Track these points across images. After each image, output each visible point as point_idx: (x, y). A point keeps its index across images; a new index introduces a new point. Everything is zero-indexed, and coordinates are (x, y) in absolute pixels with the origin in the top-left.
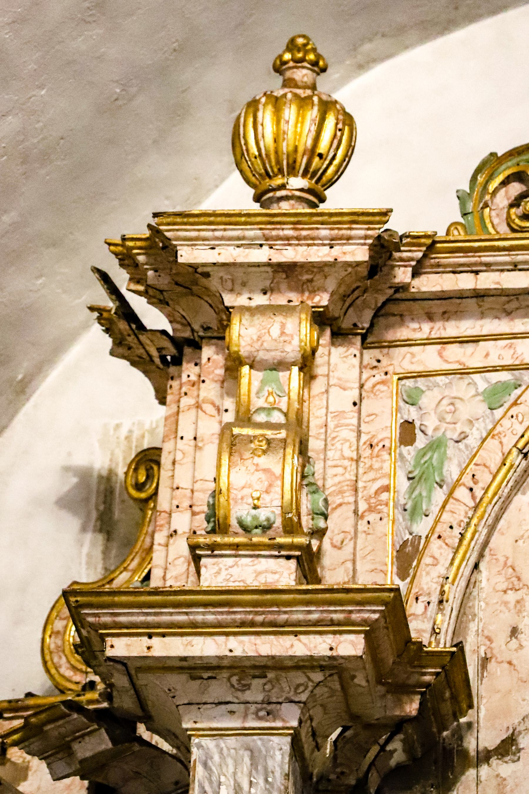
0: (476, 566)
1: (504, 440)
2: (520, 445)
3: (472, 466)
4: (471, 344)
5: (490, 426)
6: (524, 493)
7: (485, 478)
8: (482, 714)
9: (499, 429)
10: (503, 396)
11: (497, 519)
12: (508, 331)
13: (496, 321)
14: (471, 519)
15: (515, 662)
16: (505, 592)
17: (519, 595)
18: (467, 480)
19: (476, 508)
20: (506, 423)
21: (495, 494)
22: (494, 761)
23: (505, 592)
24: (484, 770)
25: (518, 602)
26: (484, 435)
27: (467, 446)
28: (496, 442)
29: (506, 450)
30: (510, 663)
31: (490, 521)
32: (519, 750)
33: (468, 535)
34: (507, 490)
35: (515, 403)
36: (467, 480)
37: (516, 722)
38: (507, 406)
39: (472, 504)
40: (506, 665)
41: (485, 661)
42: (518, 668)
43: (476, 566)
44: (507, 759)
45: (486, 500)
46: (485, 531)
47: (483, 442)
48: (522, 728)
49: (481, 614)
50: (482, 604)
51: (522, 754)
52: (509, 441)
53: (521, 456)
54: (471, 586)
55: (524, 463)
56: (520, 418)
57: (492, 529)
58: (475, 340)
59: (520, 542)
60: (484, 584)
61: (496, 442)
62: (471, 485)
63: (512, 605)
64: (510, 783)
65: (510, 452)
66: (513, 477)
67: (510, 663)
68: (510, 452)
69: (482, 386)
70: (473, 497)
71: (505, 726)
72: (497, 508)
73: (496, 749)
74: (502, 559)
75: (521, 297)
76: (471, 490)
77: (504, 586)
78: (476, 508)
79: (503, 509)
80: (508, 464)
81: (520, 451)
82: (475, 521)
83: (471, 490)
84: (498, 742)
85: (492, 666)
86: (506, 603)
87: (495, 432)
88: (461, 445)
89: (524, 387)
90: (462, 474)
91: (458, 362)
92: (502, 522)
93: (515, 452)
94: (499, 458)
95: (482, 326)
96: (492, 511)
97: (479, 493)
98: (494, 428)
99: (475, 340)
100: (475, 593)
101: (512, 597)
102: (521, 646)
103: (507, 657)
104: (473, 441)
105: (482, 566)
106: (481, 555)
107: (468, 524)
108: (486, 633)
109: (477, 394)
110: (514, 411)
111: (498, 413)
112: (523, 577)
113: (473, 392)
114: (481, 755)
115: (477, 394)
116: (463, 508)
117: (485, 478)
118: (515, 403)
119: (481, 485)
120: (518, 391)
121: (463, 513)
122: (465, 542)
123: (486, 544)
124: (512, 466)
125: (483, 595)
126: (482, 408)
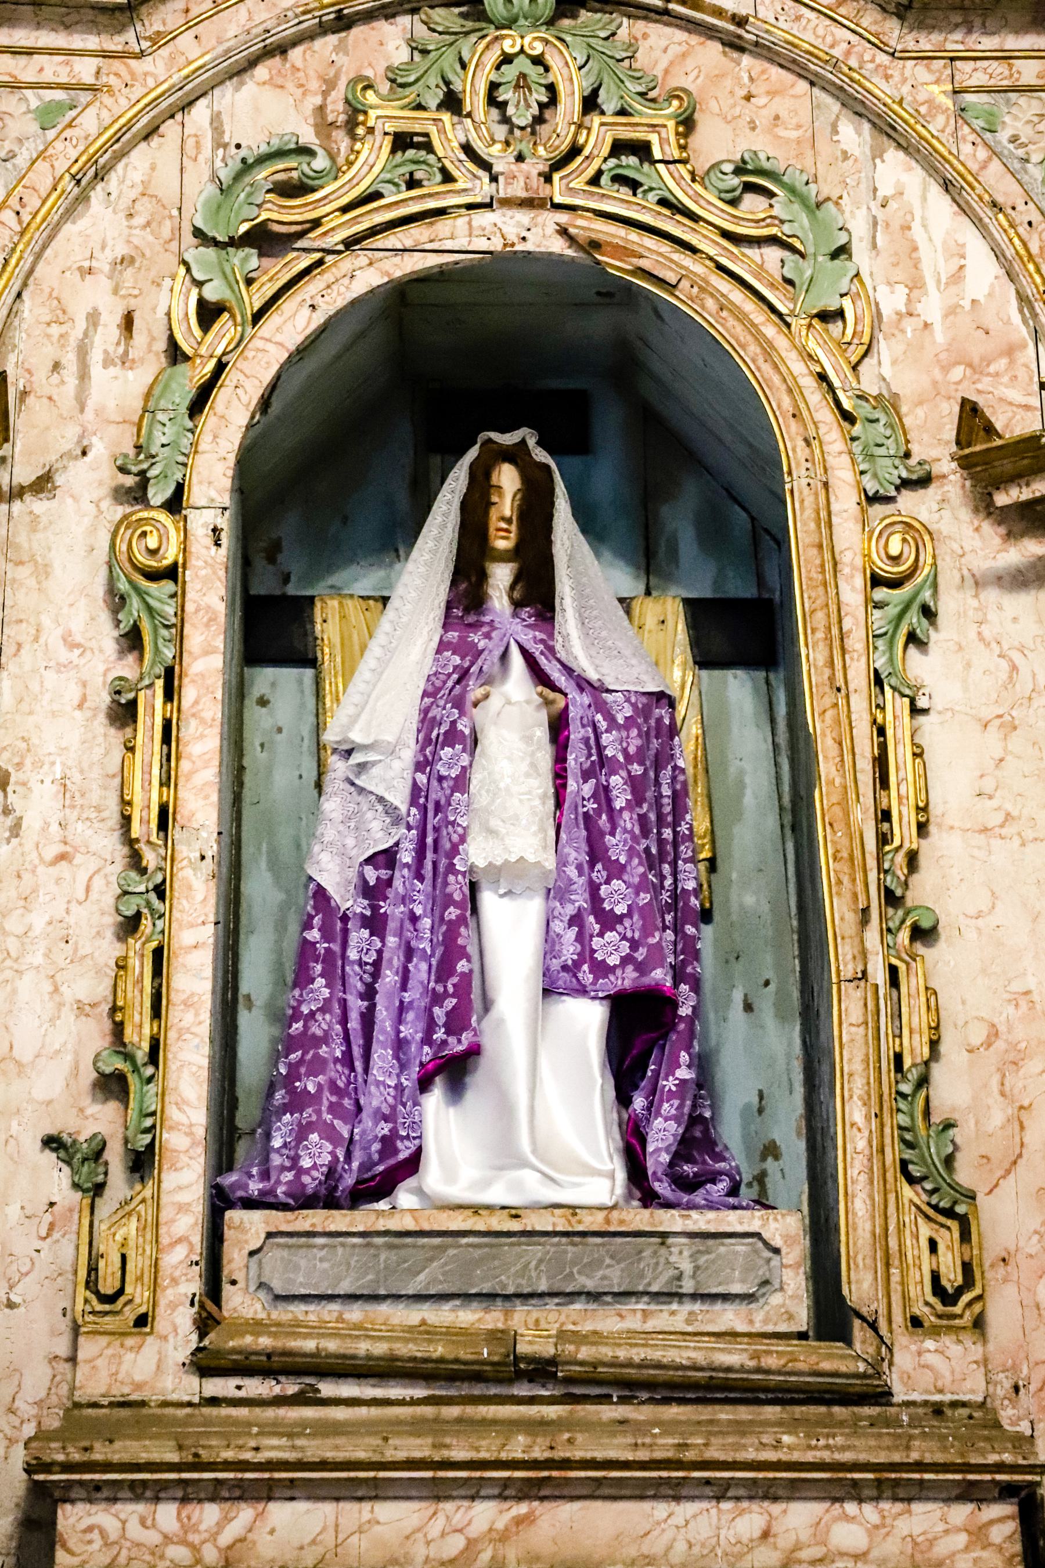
0: (19, 295)
1: (56, 164)
2: (73, 171)
3: (19, 188)
4: (24, 57)
5: (41, 148)
6: (74, 223)
7: (33, 203)
8: (17, 450)
9: (51, 151)
10: (56, 116)
11: (44, 247)
12: (66, 46)
13: (53, 34)
14: (16, 245)
15: (55, 397)
16: (48, 324)
17: (63, 329)
18: (14, 202)
19: (22, 234)
20: (59, 145)
21: (44, 220)
22: (27, 497)
23: (48, 324)
24: (17, 506)
25: (62, 336)
26: (35, 156)
27: (14, 165)
28: (47, 165)
29: (58, 175)
30: (50, 398)
31: (37, 249)
32: (55, 488)
33: (13, 262)
34: (56, 218)
35: (70, 125)
36: (14, 202)
37: (54, 458)
38: (60, 127)
39: (18, 229)
40: (45, 400)
41: (24, 394)
42: (59, 404)
43: (19, 295)
44: (42, 496)
45: (33, 226)
46: (31, 259)
47: (34, 163)
48: (59, 465)
49: (21, 346)
50: (23, 335)
51: (57, 492)
52: (62, 165)
53: (74, 182)
54: (12, 315)
55: (76, 190)
56: (74, 142)
57: (38, 256)
58: (29, 52)
59: (68, 274)
60: (26, 314)
61: (47, 165)
62: (18, 208)
63: (55, 339)
64: (44, 520)
65: (61, 178)
66: (63, 204)
67: (50, 398)
68: (61, 178)
69: (34, 103)
70: (20, 222)
71: (42, 461)
72: (45, 234)
73: (31, 486)
74: (47, 290)
75: (82, 11)
76: (18, 213)
77: (48, 319)
78: (22, 234)
79: (51, 238)
80: (59, 189)
81: (73, 177)
82: (20, 247)
83: (18, 213)
84: (34, 478)
85: (30, 400)
86: (49, 336)
87: (47, 154)
88: (9, 165)
89: (79, 109)
90: (8, 195)
91: (10, 74)
92: (48, 252)
93: (67, 177)
94: (49, 182)
95: (37, 38)
96: (39, 237)
97: (26, 218)
98: (46, 149)
99: (29, 52)
100: (16, 323)
101: (55, 330)
102: (63, 382)
103: (47, 391)
104: (22, 160)
105: (25, 295)
106: (25, 284)
107: (13, 250)
108: (26, 366)
109: (29, 111)
110: (68, 133)
111: (51, 134)
112: (69, 310)
113: (24, 109)
114: (15, 491)
115: (29, 111)
116: (8, 232)
117: (33, 203)
118: (70, 125)
119: (28, 209)
120: (73, 113)
121: (7, 238)
122: (9, 269)
123: (31, 272)
124: (63, 191)
125: (24, 326)
126: (34, 127)
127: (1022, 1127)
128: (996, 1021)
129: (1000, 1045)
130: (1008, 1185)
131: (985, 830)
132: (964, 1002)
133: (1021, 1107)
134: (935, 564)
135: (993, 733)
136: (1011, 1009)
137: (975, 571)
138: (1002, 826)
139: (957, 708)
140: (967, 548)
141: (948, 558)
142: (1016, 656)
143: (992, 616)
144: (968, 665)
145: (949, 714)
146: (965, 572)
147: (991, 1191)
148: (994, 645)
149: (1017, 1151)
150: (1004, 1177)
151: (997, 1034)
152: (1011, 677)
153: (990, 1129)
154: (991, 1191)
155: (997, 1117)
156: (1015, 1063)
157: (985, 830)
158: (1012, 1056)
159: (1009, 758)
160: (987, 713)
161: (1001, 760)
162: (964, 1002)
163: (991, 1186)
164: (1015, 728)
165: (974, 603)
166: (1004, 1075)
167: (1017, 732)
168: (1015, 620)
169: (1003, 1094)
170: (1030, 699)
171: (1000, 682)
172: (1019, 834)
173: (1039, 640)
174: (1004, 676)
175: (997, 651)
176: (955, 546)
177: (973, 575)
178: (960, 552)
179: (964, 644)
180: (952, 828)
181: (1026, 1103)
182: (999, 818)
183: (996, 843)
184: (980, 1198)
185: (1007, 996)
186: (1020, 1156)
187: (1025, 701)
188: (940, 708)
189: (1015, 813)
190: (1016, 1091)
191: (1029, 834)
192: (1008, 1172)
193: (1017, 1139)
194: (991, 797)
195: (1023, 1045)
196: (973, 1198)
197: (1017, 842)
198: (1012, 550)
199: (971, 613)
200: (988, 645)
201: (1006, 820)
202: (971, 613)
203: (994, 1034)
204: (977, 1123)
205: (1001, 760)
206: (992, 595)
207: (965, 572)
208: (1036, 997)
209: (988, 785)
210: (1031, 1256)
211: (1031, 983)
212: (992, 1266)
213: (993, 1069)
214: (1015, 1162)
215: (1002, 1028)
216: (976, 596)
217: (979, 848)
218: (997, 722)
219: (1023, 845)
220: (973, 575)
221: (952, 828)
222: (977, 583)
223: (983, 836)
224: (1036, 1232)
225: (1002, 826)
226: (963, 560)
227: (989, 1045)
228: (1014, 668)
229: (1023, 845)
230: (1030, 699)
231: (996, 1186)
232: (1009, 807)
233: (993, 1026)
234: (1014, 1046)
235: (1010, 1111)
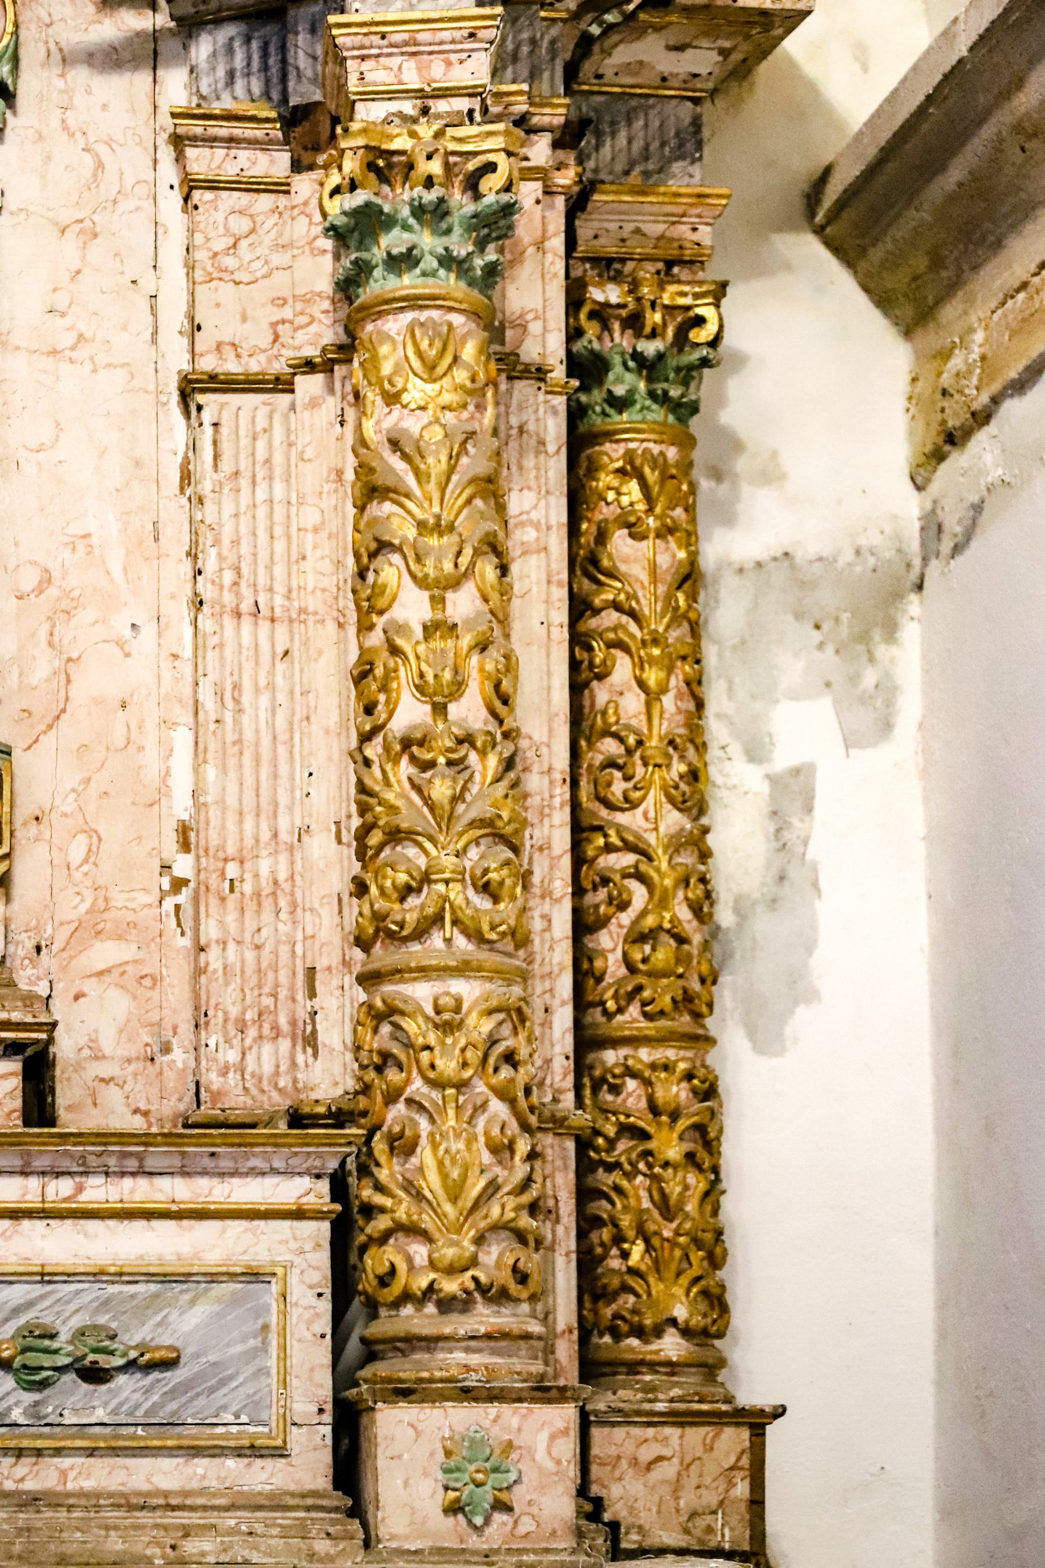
127: (69, 681)
128: (50, 565)
129: (52, 592)
130: (48, 741)
131: (54, 352)
132: (16, 544)
133: (69, 660)
134: (16, 33)
135: (71, 242)
136: (67, 554)
137: (63, 45)
138: (73, 348)
139: (32, 209)
140: (56, 17)
141: (33, 27)
142: (103, 150)
143: (79, 100)
144: (49, 158)
145: (23, 215)
146: (52, 46)
147: (29, 747)
148: (78, 135)
149: (61, 706)
150: (45, 732)
151: (50, 581)
152: (95, 175)
153: (34, 682)
154: (29, 747)
155: (43, 668)
156: (68, 613)
157: (54, 352)
158: (65, 604)
159: (86, 270)
160: (66, 216)
161: (78, 272)
162: (16, 544)
163: (29, 742)
164: (96, 235)
165: (60, 83)
166: (53, 626)
167: (99, 239)
168: (105, 106)
169: (50, 644)
170: (115, 202)
171: (83, 181)
172: (91, 358)
173: (129, 133)
174: (88, 173)
175: (82, 144)
176: (43, 14)
177: (61, 50)
178: (48, 20)
179: (45, 133)
180: (18, 348)
181: (75, 656)
182: (70, 339)
183: (65, 368)
184: (16, 754)
185: (66, 539)
186: (64, 711)
187: (109, 205)
188: (13, 207)
189: (88, 335)
190: (65, 642)
191: (102, 359)
192: (50, 727)
193: (63, 693)
194: (63, 315)
195: (77, 592)
196: (9, 754)
197: (88, 366)
198: (107, 21)
199: (55, 95)
200: (72, 135)
201: (78, 342)
202: (55, 95)
203: (47, 580)
204: (21, 675)
205: (78, 272)
206: (80, 75)
207: (52, 46)
208: (94, 541)
209: (61, 301)
210: (65, 815)
211: (91, 526)
212: (25, 824)
213: (43, 617)
214: (58, 717)
215: (56, 574)
216: (62, 75)
217: (45, 372)
218: (77, 227)
219: (95, 371)
220: (61, 50)
221: (18, 348)
222: (64, 60)
223: (51, 359)
224: (73, 790)
225: (73, 348)
226: (50, 31)
227: (41, 592)
228: (100, 165)
229: (95, 371)
230: (115, 202)
231: (36, 741)
232: (82, 326)
233: (47, 571)
234: (67, 594)
235: (57, 663)
